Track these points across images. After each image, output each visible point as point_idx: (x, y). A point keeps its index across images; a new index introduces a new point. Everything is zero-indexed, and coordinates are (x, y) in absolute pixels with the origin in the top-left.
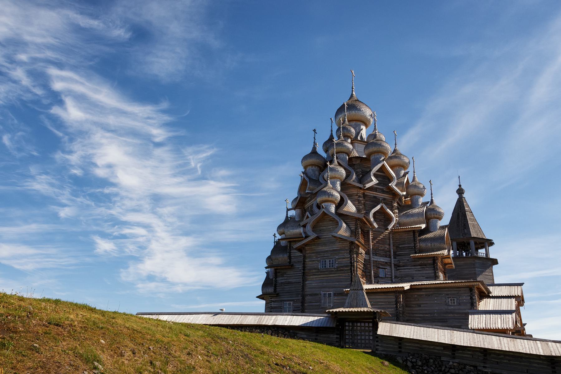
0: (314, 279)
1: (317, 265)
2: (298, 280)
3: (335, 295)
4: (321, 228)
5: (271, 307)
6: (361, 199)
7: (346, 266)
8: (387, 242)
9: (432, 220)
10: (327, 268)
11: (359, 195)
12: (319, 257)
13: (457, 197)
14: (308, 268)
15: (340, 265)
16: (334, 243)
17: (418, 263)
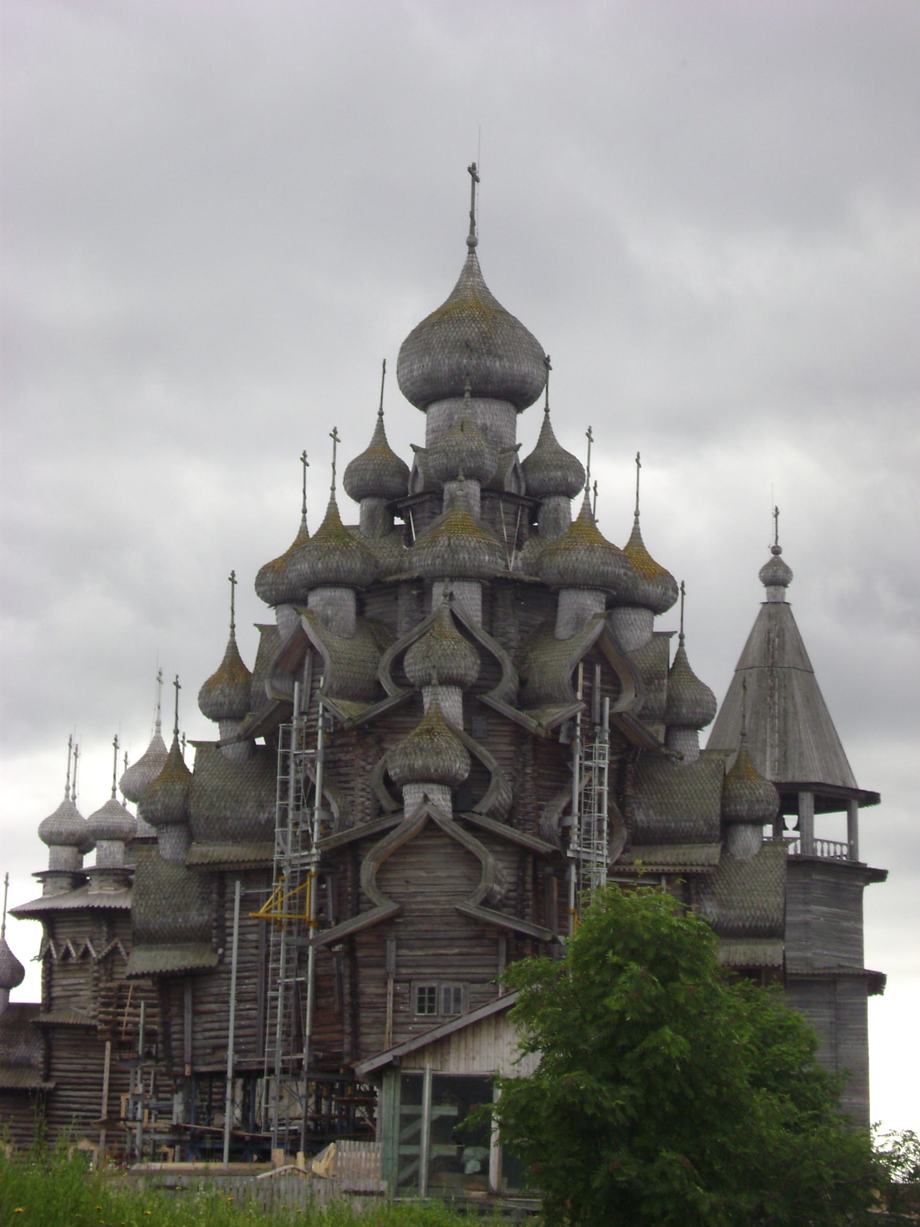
13: (761, 593)
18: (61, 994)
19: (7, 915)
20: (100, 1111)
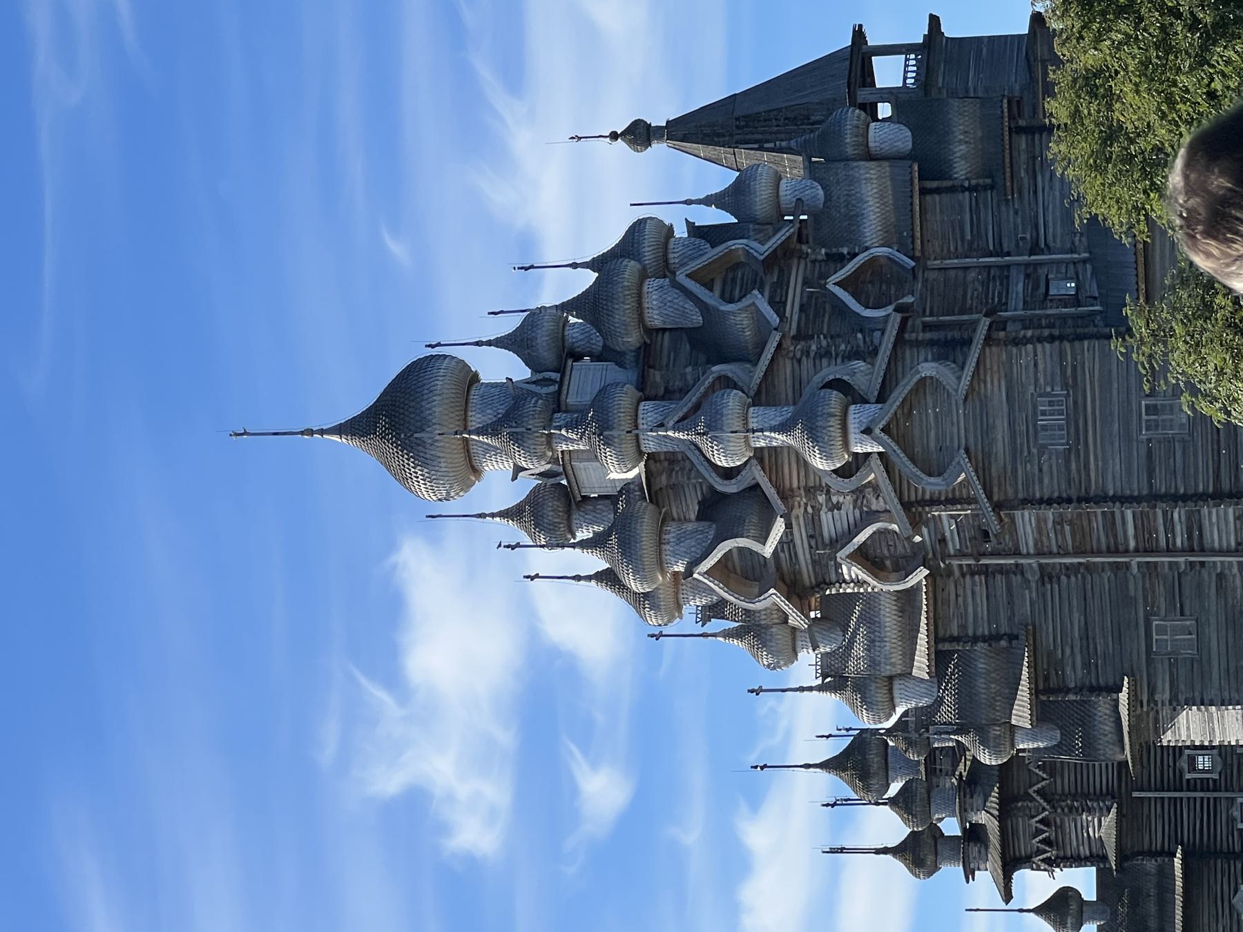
0: (1100, 464)
1: (1054, 457)
2: (1075, 602)
4: (932, 445)
5: (1170, 704)
6: (814, 347)
7: (1062, 355)
8: (956, 276)
9: (871, 144)
10: (1067, 419)
11: (798, 355)
12: (1029, 452)
13: (660, 149)
16: (986, 396)
17: (1026, 180)
19: (1009, 907)
20: (1202, 799)
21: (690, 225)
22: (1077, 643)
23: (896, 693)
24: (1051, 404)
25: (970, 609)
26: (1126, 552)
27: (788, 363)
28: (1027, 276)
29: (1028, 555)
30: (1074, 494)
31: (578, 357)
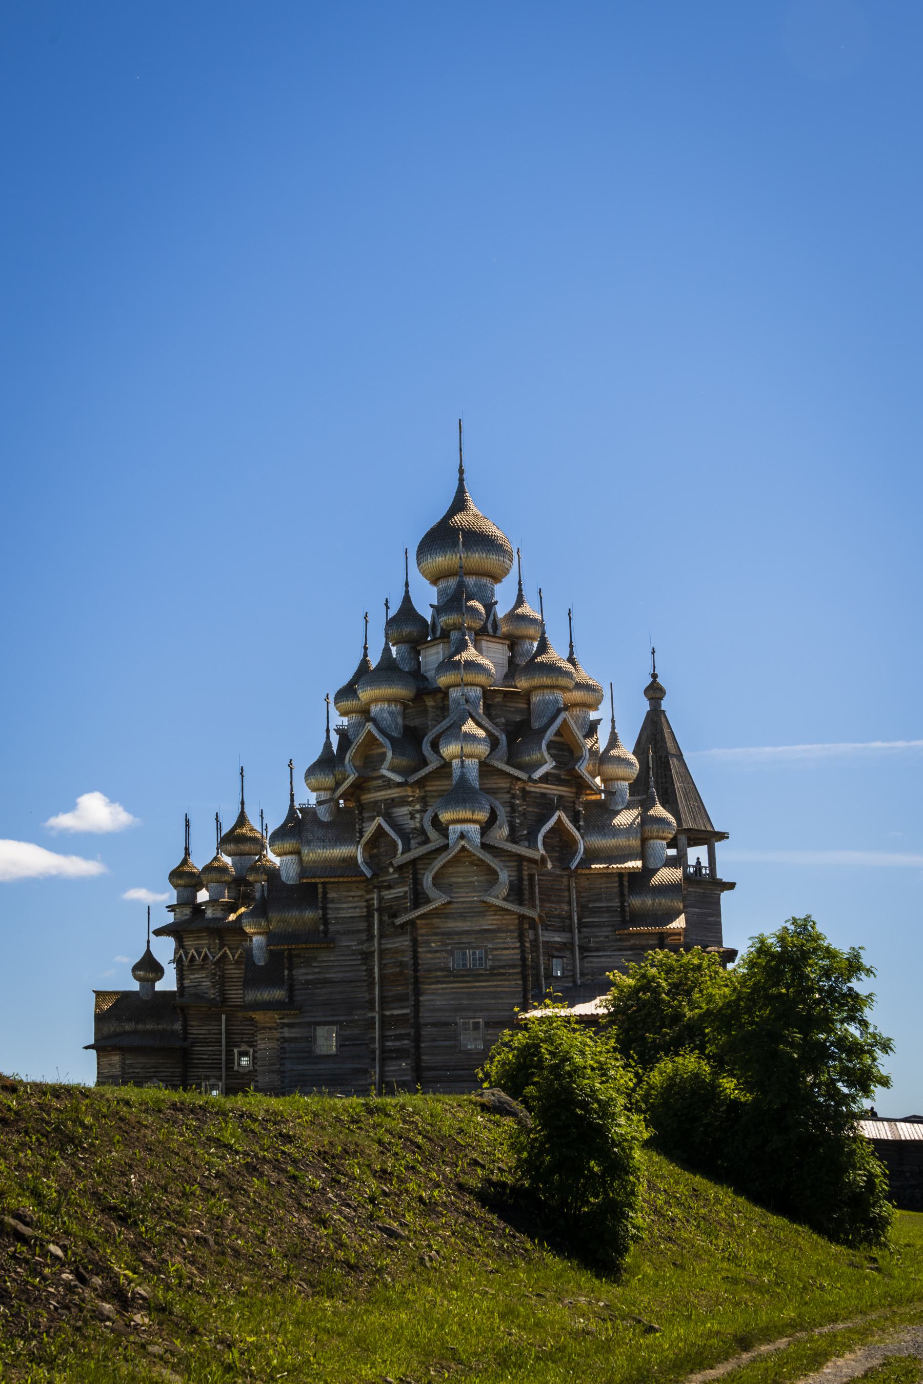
0: (440, 991)
1: (445, 960)
2: (349, 974)
3: (487, 1025)
5: (282, 1038)
6: (518, 802)
7: (513, 966)
8: (565, 897)
9: (651, 841)
10: (470, 969)
11: (513, 792)
12: (449, 944)
13: (646, 706)
14: (425, 967)
15: (496, 963)
16: (485, 916)
17: (628, 944)
18: (190, 984)
19: (151, 934)
20: (221, 1059)
21: (598, 722)
22: (322, 976)
23: (289, 857)
24: (481, 959)
25: (344, 906)
26: (382, 1008)
27: (508, 785)
28: (564, 944)
29: (380, 944)
30: (420, 973)
31: (511, 648)
